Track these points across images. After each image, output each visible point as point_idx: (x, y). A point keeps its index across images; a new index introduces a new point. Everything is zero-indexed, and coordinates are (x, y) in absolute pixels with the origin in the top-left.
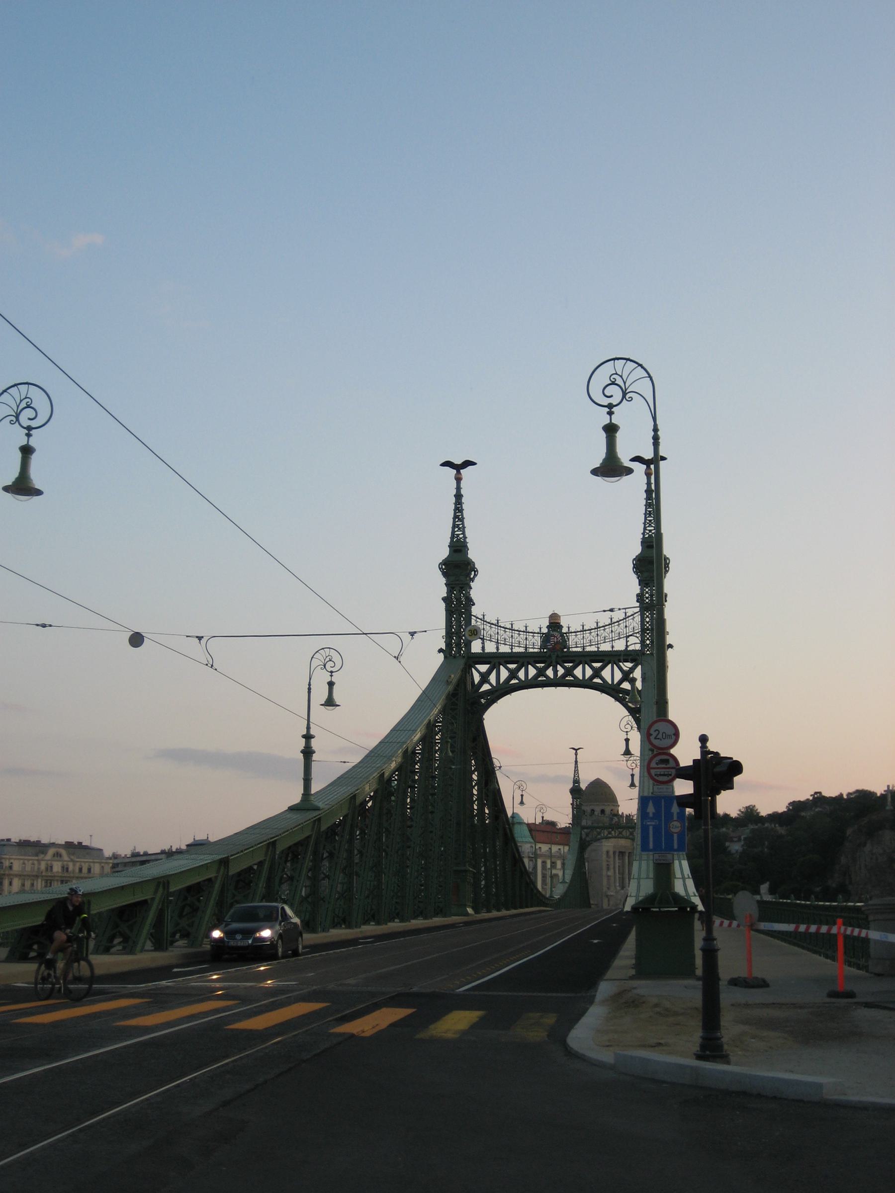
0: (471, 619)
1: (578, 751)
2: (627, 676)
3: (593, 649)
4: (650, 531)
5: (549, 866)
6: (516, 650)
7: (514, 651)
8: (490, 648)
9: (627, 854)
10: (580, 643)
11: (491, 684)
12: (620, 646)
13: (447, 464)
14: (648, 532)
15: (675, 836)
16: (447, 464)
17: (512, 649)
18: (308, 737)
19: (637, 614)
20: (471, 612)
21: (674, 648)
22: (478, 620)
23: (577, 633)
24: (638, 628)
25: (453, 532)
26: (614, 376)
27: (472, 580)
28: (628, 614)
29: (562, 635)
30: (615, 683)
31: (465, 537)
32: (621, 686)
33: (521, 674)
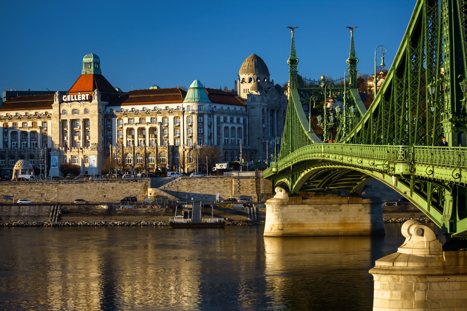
5: (222, 120)
9: (276, 111)
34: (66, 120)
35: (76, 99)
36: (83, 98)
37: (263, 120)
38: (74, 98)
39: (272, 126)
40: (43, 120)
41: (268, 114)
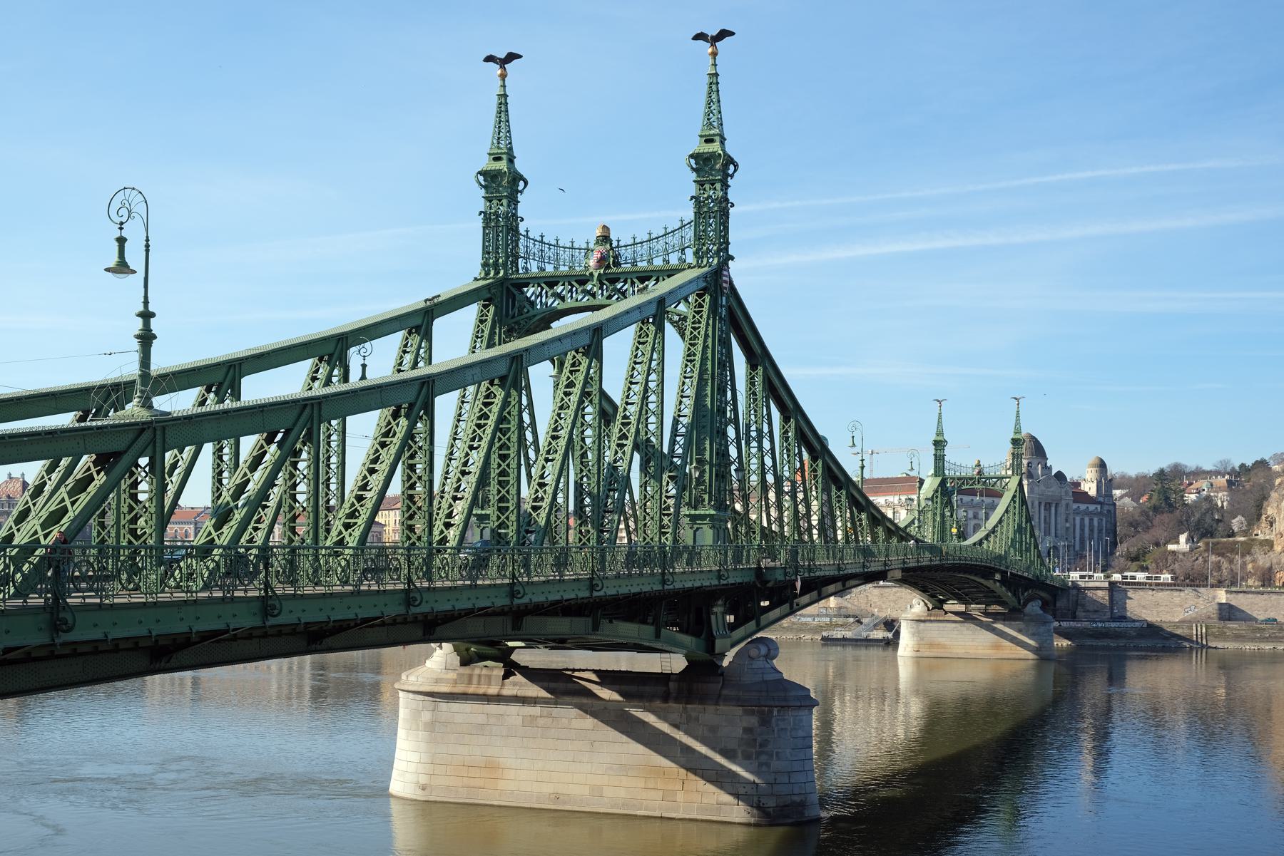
3: (645, 264)
6: (564, 269)
8: (534, 267)
12: (674, 260)
13: (490, 59)
16: (490, 59)
19: (693, 223)
27: (521, 192)
28: (684, 223)
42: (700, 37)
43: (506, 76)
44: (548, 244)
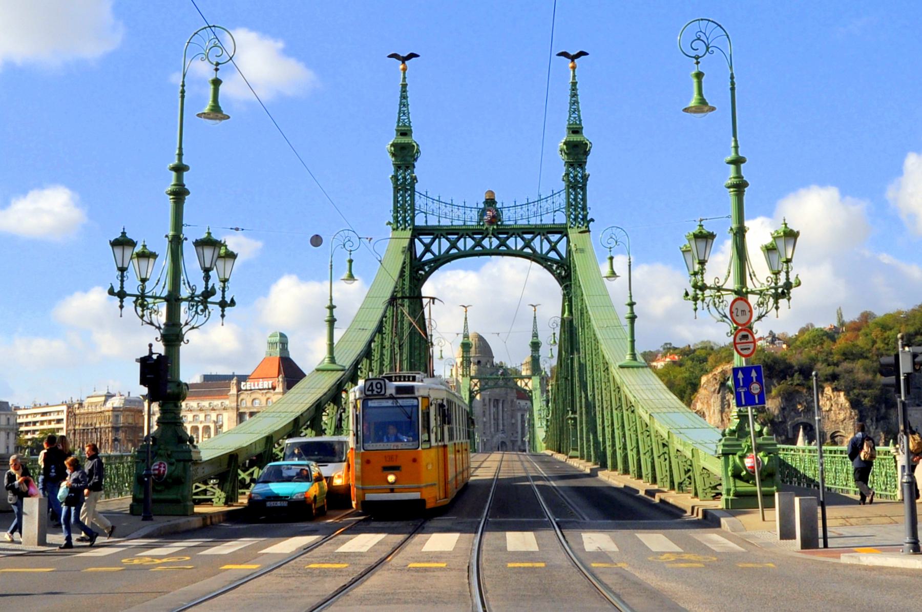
0: (414, 194)
1: (468, 308)
2: (553, 248)
3: (525, 222)
4: (575, 118)
6: (456, 223)
7: (454, 224)
8: (433, 222)
9: (501, 402)
10: (513, 217)
11: (433, 254)
14: (572, 119)
15: (756, 396)
17: (452, 222)
18: (331, 308)
20: (414, 188)
21: (595, 222)
22: (421, 196)
23: (510, 208)
24: (564, 204)
25: (399, 117)
26: (699, 33)
28: (555, 192)
29: (497, 210)
30: (544, 253)
31: (410, 122)
32: (549, 255)
33: (460, 244)
34: (244, 413)
35: (257, 388)
36: (266, 386)
37: (484, 412)
38: (254, 385)
39: (496, 420)
40: (218, 412)
41: (490, 405)
42: (564, 54)
43: (406, 70)
44: (444, 203)
